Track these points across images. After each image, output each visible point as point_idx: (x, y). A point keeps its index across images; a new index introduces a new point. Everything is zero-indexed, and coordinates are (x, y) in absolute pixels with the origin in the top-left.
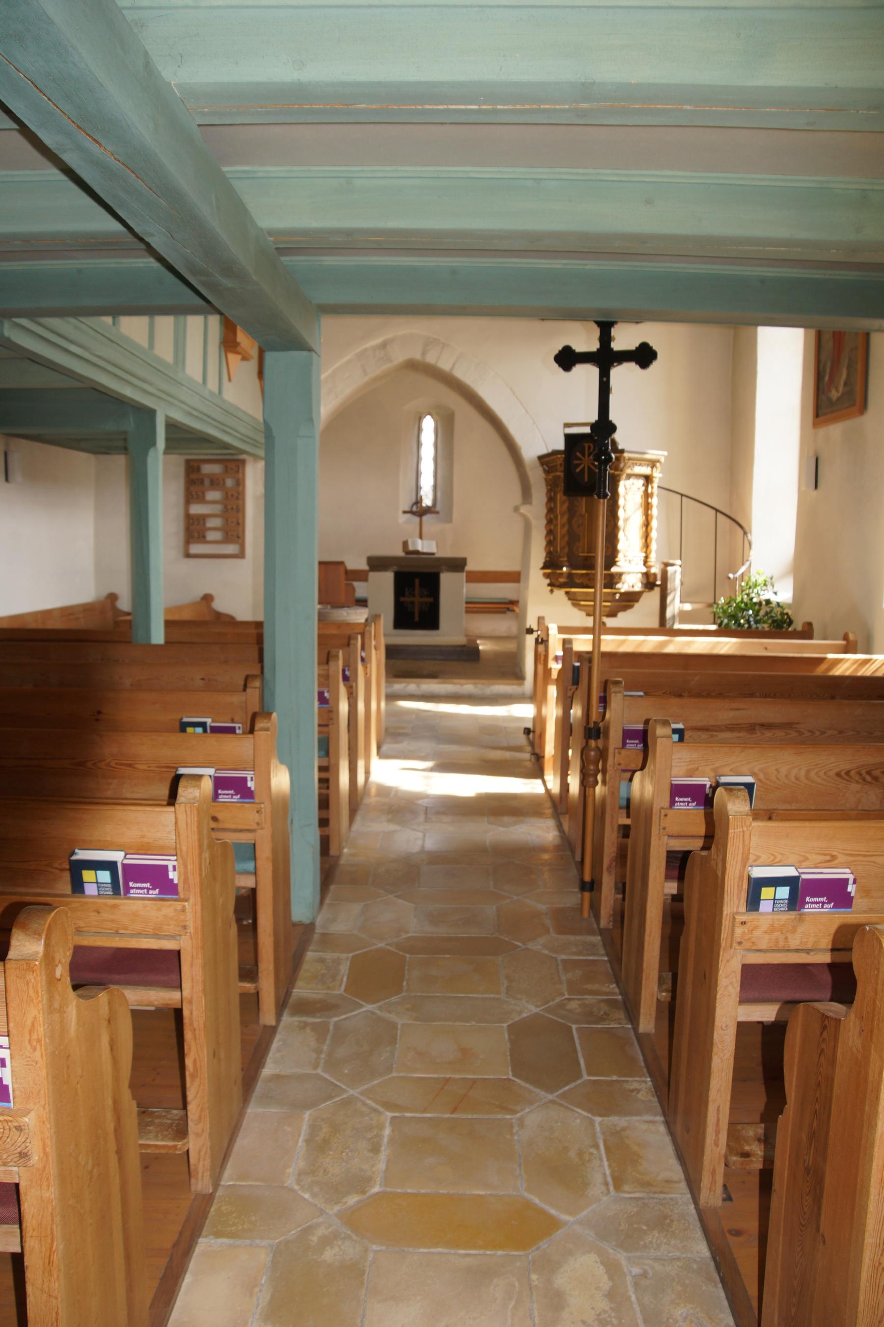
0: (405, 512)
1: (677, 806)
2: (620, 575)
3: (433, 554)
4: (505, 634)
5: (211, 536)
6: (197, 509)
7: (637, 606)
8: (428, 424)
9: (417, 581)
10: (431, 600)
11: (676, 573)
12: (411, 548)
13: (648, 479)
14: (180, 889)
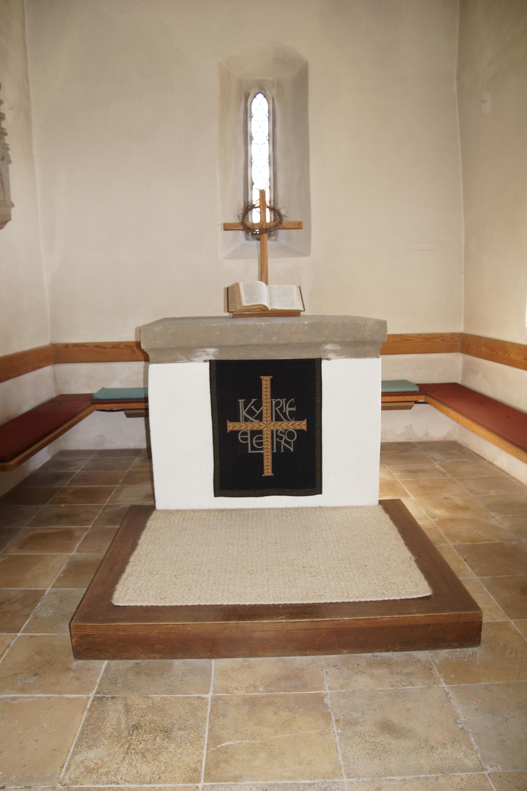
0: (227, 227)
3: (295, 314)
4: (402, 439)
8: (260, 106)
9: (266, 381)
10: (303, 425)
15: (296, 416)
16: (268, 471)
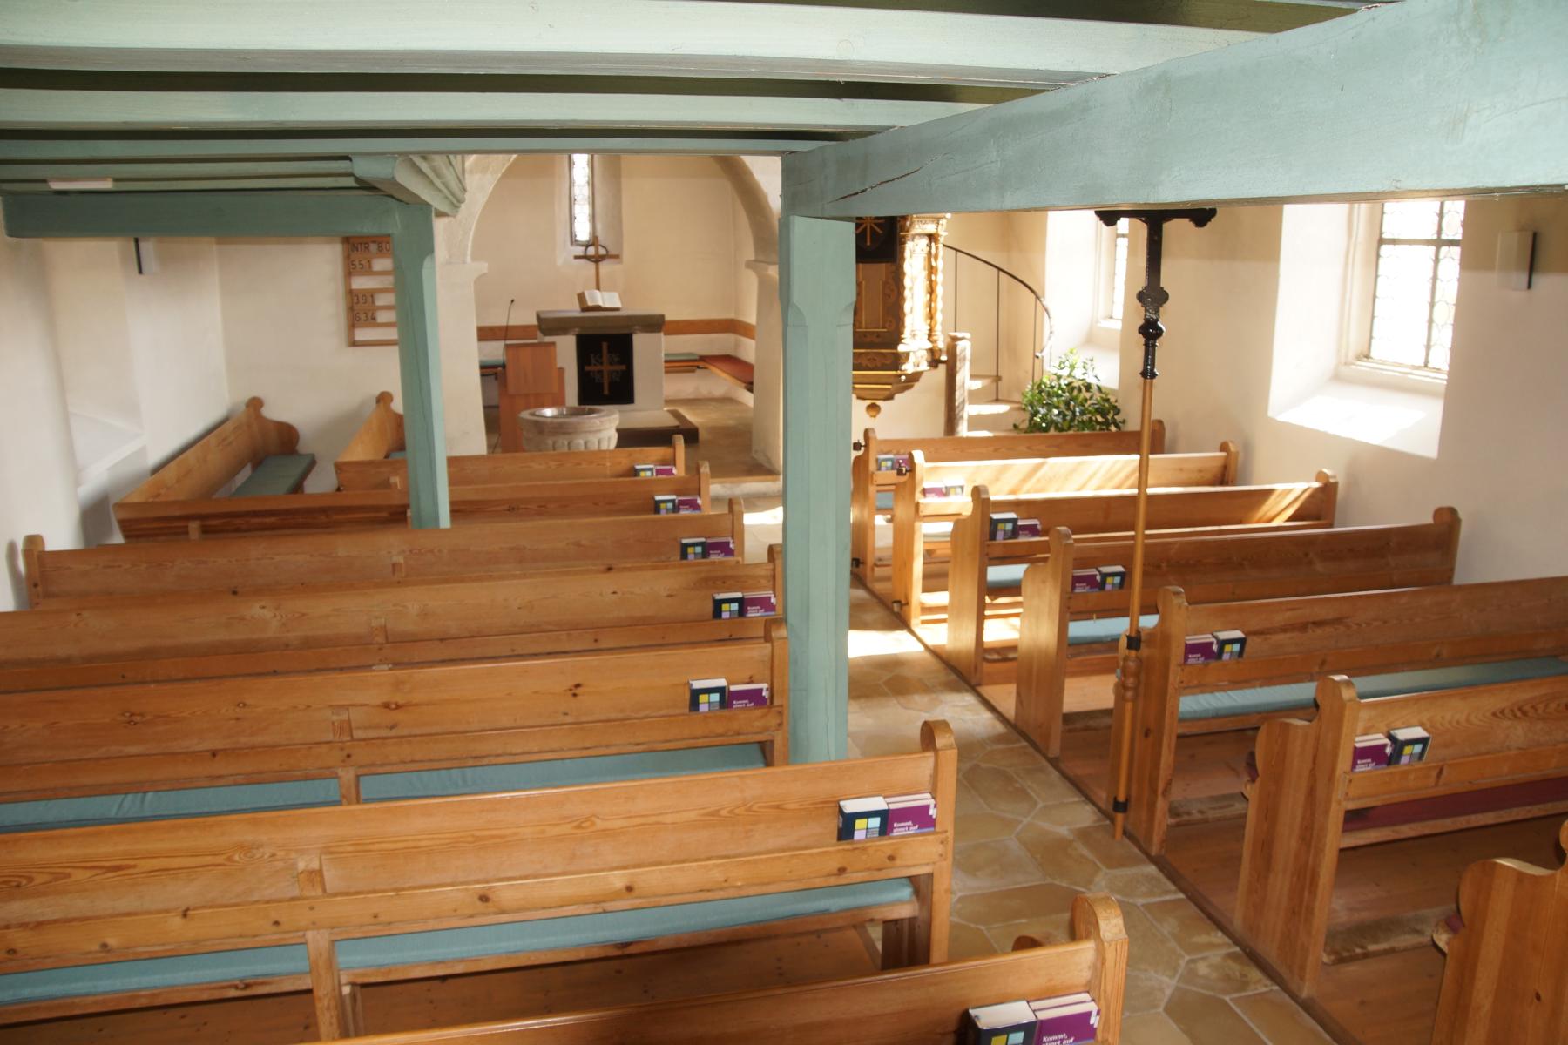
1: (1358, 769)
2: (907, 355)
3: (617, 309)
5: (382, 317)
6: (360, 283)
7: (917, 385)
9: (605, 345)
10: (623, 367)
11: (965, 348)
12: (590, 303)
13: (932, 238)
14: (1099, 1033)
15: (620, 363)
16: (606, 392)
